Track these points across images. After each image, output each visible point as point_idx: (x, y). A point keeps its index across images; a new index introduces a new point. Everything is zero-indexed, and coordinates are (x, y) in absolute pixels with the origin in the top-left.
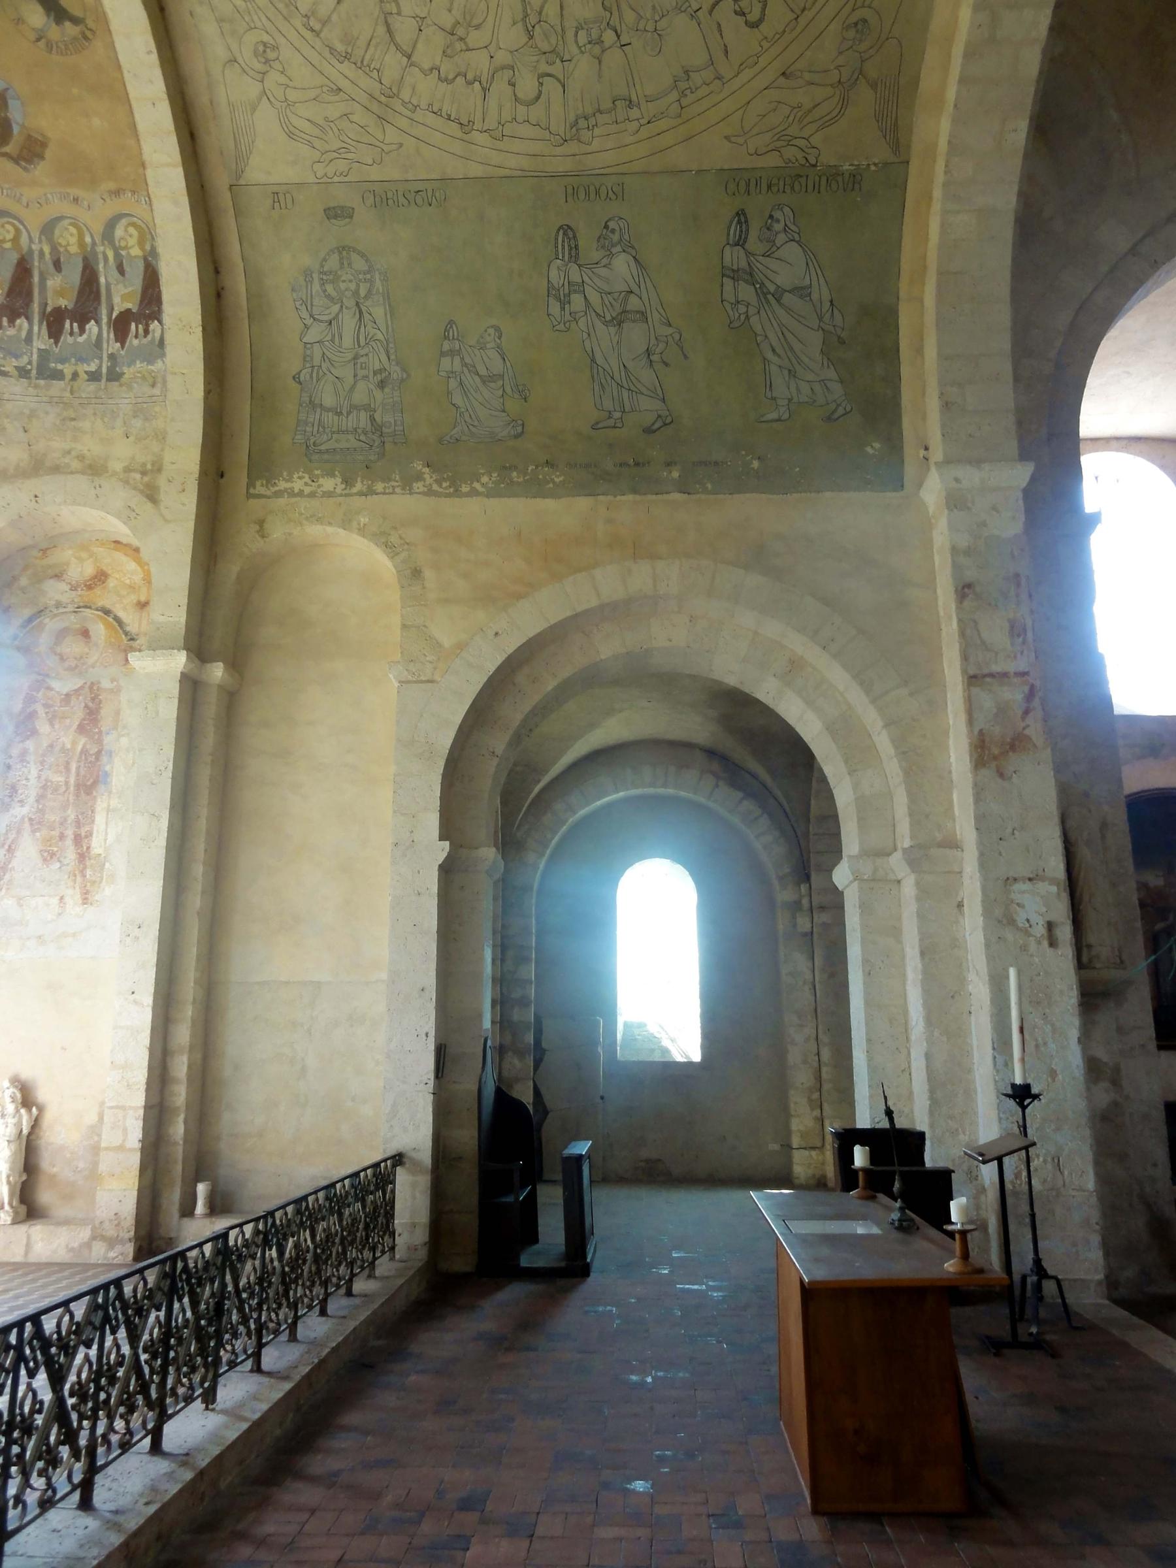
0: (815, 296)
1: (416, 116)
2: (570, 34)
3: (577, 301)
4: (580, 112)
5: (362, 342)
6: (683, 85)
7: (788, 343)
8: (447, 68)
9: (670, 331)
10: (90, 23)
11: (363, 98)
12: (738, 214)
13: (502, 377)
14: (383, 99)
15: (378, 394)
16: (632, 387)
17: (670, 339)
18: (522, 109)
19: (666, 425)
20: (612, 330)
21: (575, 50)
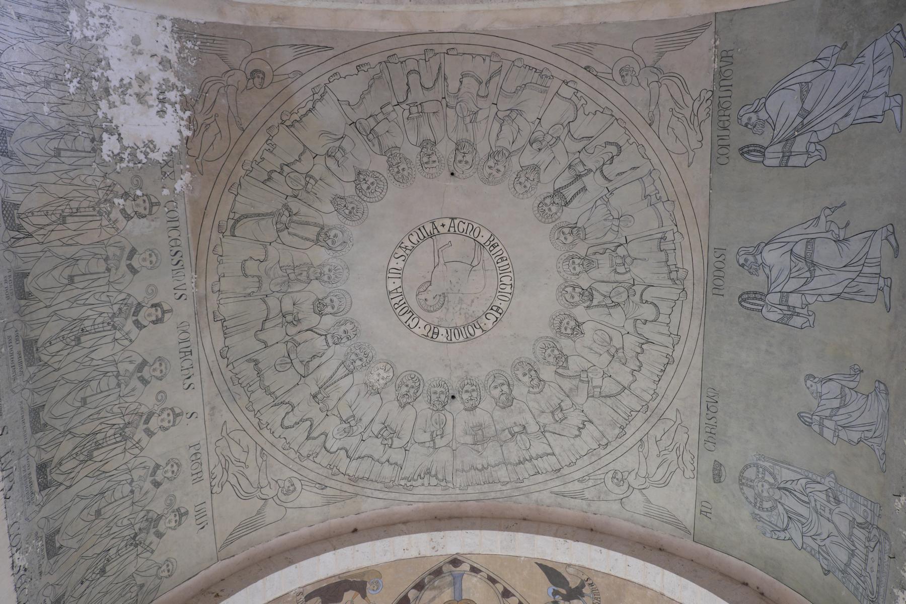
0: (808, 78)
1: (661, 395)
2: (619, 278)
3: (794, 300)
4: (666, 275)
5: (806, 499)
6: (654, 200)
7: (842, 101)
8: (633, 365)
9: (823, 218)
10: (585, 577)
11: (647, 427)
12: (742, 154)
13: (843, 386)
14: (649, 413)
15: (844, 508)
16: (862, 262)
17: (829, 218)
18: (662, 318)
19: (893, 233)
20: (818, 272)
21: (628, 276)
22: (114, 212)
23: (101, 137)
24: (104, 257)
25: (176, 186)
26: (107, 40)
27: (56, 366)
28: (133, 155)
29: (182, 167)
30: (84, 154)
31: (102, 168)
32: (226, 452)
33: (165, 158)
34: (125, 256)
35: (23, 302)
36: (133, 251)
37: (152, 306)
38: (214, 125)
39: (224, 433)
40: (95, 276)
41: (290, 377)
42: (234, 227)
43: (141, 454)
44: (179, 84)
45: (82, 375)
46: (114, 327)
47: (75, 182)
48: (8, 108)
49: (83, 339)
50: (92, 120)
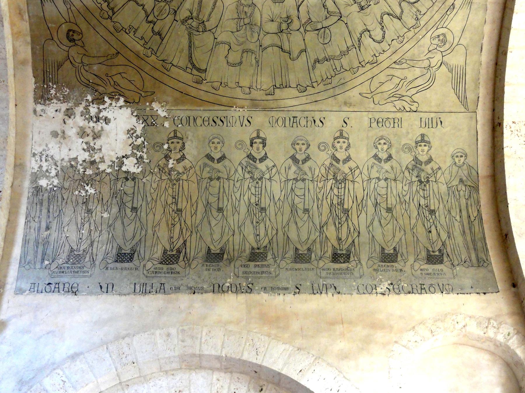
22: (177, 169)
23: (125, 172)
24: (209, 181)
25: (163, 115)
26: (57, 158)
27: (274, 232)
28: (138, 148)
29: (148, 109)
30: (136, 188)
31: (147, 174)
32: (386, 95)
33: (141, 122)
34: (210, 163)
35: (225, 256)
36: (209, 157)
37: (251, 146)
38: (115, 78)
39: (369, 96)
40: (222, 190)
41: (338, 31)
42: (199, 70)
43: (361, 168)
44: (84, 104)
45: (287, 209)
46: (261, 179)
47: (155, 198)
48: (104, 248)
49: (263, 206)
50: (113, 178)
